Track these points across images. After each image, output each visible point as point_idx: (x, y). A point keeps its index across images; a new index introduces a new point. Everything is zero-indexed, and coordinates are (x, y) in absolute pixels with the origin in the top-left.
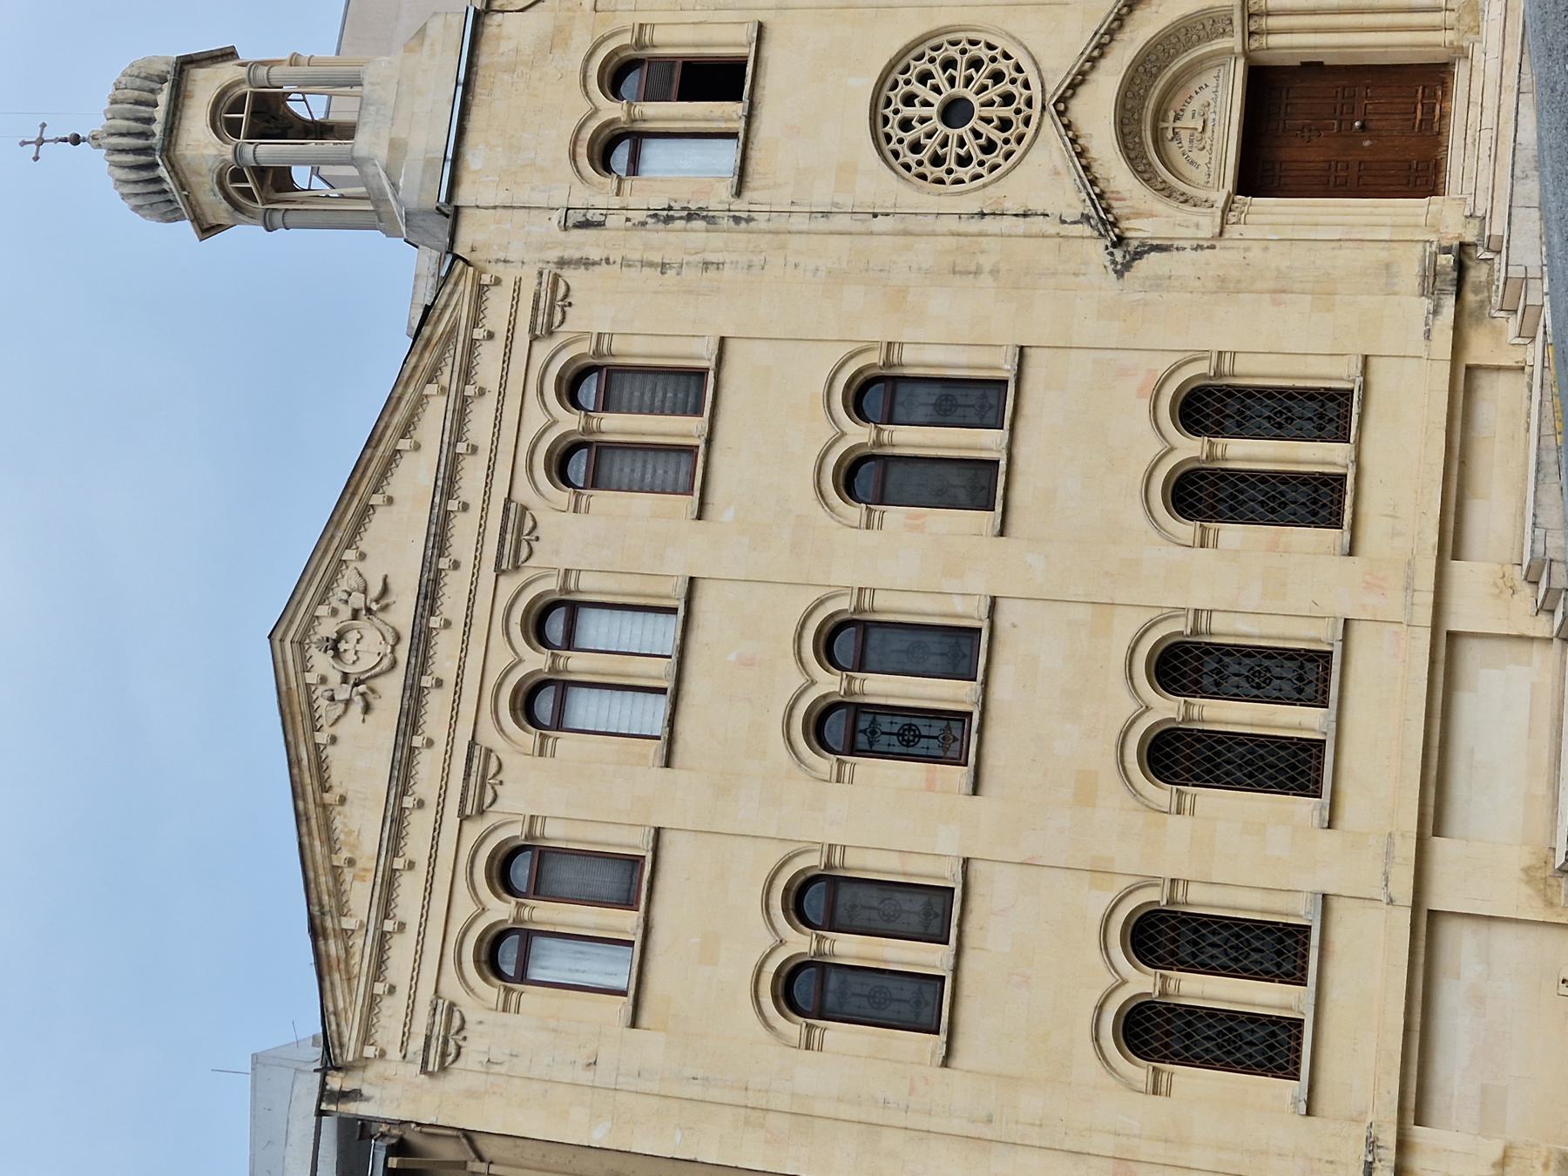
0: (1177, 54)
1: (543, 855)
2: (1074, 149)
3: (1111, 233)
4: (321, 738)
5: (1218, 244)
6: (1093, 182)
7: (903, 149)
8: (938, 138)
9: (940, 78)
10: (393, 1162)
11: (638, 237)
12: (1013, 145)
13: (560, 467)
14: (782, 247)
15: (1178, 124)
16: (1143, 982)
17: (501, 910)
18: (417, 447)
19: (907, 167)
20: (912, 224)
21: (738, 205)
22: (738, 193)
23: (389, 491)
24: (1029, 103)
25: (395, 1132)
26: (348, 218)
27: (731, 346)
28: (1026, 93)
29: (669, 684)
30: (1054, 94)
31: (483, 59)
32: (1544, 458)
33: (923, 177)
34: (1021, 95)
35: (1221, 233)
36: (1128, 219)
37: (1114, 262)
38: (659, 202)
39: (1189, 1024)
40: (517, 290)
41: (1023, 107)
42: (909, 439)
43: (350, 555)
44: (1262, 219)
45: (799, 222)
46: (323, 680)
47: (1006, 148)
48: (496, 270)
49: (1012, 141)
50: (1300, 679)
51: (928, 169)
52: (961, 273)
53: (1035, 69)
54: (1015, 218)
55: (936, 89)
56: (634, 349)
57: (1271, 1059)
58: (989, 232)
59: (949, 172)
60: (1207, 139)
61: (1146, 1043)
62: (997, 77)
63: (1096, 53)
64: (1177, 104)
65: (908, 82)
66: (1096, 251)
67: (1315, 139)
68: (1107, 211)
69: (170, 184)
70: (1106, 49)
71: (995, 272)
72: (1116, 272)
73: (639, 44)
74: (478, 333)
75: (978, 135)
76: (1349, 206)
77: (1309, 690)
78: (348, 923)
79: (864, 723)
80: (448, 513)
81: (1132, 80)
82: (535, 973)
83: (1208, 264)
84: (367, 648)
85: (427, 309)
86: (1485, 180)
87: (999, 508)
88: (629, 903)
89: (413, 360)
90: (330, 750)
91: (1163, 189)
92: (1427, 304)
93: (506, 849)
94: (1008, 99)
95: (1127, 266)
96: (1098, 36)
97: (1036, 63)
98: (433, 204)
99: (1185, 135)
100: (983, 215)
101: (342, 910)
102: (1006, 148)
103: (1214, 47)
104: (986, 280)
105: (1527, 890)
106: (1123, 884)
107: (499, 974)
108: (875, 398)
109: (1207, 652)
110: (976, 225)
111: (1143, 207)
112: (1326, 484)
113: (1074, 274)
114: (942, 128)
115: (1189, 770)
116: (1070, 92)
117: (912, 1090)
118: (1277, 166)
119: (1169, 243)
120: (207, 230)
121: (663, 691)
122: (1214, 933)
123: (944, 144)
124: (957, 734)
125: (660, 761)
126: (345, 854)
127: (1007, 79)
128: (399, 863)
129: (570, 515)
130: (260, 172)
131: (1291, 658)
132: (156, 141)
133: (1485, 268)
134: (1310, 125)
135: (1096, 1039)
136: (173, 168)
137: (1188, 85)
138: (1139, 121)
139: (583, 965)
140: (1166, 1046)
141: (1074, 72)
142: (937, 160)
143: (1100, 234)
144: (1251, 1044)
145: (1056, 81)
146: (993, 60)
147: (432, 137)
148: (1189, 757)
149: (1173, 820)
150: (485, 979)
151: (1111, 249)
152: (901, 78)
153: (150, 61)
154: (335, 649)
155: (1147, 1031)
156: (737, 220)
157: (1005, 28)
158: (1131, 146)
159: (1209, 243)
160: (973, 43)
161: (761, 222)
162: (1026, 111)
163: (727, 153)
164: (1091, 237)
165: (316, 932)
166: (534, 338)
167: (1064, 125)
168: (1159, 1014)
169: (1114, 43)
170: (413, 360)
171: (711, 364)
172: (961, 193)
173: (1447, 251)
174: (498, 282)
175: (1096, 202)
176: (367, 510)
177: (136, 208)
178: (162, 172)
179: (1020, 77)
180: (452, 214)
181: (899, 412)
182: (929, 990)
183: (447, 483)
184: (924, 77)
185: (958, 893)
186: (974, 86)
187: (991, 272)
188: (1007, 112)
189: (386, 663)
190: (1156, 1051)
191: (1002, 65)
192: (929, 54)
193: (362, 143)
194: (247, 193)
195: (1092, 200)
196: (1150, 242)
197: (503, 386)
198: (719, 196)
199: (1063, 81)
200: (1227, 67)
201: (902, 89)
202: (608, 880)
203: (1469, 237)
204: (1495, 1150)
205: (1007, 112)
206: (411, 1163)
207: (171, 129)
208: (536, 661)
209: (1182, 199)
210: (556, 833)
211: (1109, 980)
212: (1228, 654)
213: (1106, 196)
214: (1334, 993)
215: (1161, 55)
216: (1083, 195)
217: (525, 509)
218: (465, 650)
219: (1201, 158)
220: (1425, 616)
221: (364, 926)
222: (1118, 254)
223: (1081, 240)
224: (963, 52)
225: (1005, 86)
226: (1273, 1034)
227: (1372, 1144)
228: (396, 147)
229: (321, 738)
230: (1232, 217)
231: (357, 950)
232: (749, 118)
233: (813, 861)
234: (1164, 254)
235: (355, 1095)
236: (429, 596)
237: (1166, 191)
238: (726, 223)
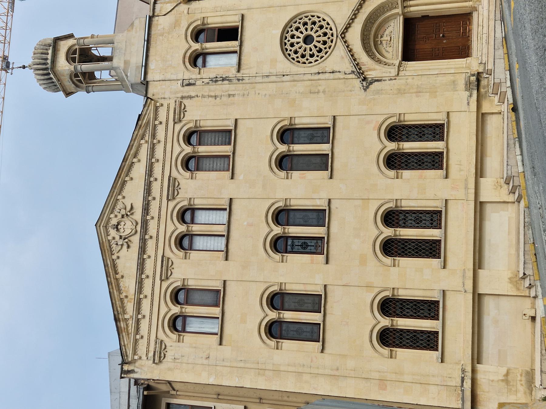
0: (380, 15)
1: (188, 291)
2: (348, 49)
3: (362, 77)
4: (114, 257)
5: (397, 78)
6: (355, 60)
7: (292, 53)
8: (303, 49)
9: (303, 29)
10: (145, 393)
11: (206, 88)
13: (186, 164)
14: (254, 88)
15: (382, 39)
16: (385, 322)
17: (176, 310)
18: (139, 161)
19: (293, 59)
20: (296, 77)
21: (239, 75)
22: (239, 71)
23: (131, 175)
24: (332, 35)
25: (146, 382)
26: (113, 87)
27: (239, 122)
28: (331, 32)
29: (225, 233)
30: (340, 31)
31: (153, 32)
32: (510, 142)
33: (299, 62)
34: (329, 33)
35: (398, 74)
36: (367, 71)
37: (363, 86)
38: (213, 75)
39: (401, 335)
40: (168, 107)
41: (330, 36)
42: (299, 148)
43: (120, 197)
44: (411, 69)
45: (259, 79)
46: (114, 238)
47: (325, 50)
48: (162, 101)
49: (327, 48)
50: (432, 220)
51: (300, 59)
52: (313, 93)
53: (333, 24)
54: (330, 74)
55: (302, 33)
56: (208, 124)
57: (428, 345)
58: (322, 79)
59: (307, 59)
60: (392, 43)
61: (387, 342)
62: (321, 27)
63: (353, 17)
64: (381, 32)
65: (292, 31)
66: (357, 83)
67: (427, 41)
68: (360, 69)
69: (55, 80)
70: (357, 16)
71: (324, 92)
72: (364, 89)
73: (203, 24)
74: (157, 122)
75: (316, 47)
76: (440, 63)
77: (435, 223)
78: (127, 316)
79: (290, 242)
80: (150, 182)
81: (366, 25)
82: (188, 329)
83: (394, 85)
84: (127, 227)
85: (140, 115)
86: (485, 51)
87: (330, 170)
88: (217, 305)
89: (136, 132)
90: (117, 261)
91: (378, 61)
92: (468, 93)
93: (176, 290)
94: (325, 34)
95: (368, 87)
96: (354, 11)
97: (334, 22)
98: (139, 81)
99: (384, 42)
100: (319, 73)
101: (124, 312)
102: (325, 50)
103: (392, 13)
104: (321, 95)
105: (510, 285)
106: (377, 290)
107: (177, 330)
108: (287, 136)
109: (401, 213)
110: (317, 77)
111: (372, 67)
112: (437, 155)
113: (350, 91)
114: (304, 45)
115: (397, 252)
116: (346, 30)
117: (312, 361)
118: (416, 51)
119: (381, 78)
120: (68, 94)
121: (223, 236)
122: (408, 305)
123: (305, 50)
124: (320, 244)
125: (224, 258)
126: (124, 294)
127: (324, 28)
128: (142, 296)
129: (190, 180)
130: (84, 74)
131: (428, 213)
132: (49, 66)
133: (486, 80)
134: (425, 37)
135: (371, 341)
136: (55, 75)
137: (384, 26)
138: (369, 39)
139: (203, 326)
140: (394, 342)
141: (346, 23)
142: (303, 56)
143: (358, 77)
144: (422, 340)
145: (340, 28)
147: (137, 59)
148: (396, 248)
149: (392, 269)
150: (172, 332)
151: (362, 82)
152: (290, 30)
153: (45, 40)
154: (117, 228)
155: (387, 338)
156: (239, 80)
157: (324, 11)
158: (367, 47)
159: (394, 78)
160: (313, 16)
161: (246, 80)
163: (234, 59)
164: (355, 78)
165: (117, 320)
166: (175, 123)
167: (344, 42)
168: (391, 332)
169: (359, 13)
170: (136, 132)
171: (232, 128)
172: (312, 66)
173: (473, 75)
174: (162, 105)
175: (356, 66)
176: (124, 183)
177: (45, 88)
178: (52, 76)
179: (329, 27)
180: (146, 84)
181: (296, 140)
182: (315, 328)
183: (150, 172)
184: (297, 29)
185: (323, 296)
186: (314, 30)
187: (323, 92)
188: (325, 38)
189: (133, 231)
190: (390, 344)
191: (323, 23)
192: (298, 21)
193: (116, 62)
194: (80, 81)
195: (355, 66)
196: (374, 79)
197: (166, 139)
198: (232, 73)
199: (343, 27)
200: (397, 19)
201: (290, 33)
202: (209, 298)
203: (480, 71)
204: (504, 371)
205: (325, 38)
206: (152, 393)
207: (54, 61)
208: (182, 228)
209: (384, 64)
210: (192, 284)
211: (374, 322)
212: (408, 213)
213: (359, 64)
214: (448, 323)
215: (375, 17)
216: (352, 64)
217: (175, 179)
218: (159, 226)
219: (389, 50)
220: (472, 197)
221: (132, 317)
222: (364, 83)
223: (352, 79)
224: (310, 19)
225: (324, 30)
226: (429, 337)
227: (463, 371)
228: (126, 63)
229: (114, 257)
230: (401, 69)
231: (130, 325)
232: (241, 46)
233: (276, 288)
234: (379, 82)
235: (132, 371)
236: (146, 209)
237: (379, 61)
238: (235, 81)
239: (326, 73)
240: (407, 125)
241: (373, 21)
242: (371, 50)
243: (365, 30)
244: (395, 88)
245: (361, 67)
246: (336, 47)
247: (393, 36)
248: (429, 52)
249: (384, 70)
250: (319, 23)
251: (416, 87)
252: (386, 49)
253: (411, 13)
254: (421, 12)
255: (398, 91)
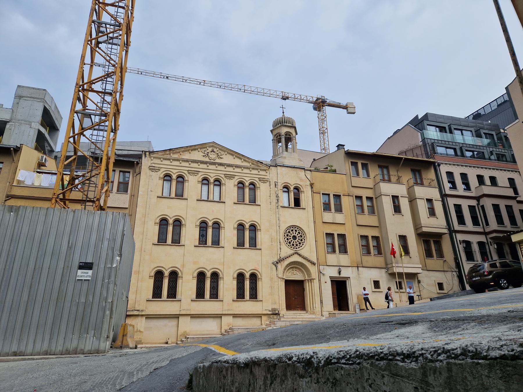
1: (183, 182)
4: (199, 150)
6: (285, 258)
7: (289, 230)
8: (291, 235)
9: (299, 235)
10: (135, 162)
11: (274, 192)
12: (290, 246)
13: (240, 183)
14: (274, 213)
16: (167, 273)
17: (174, 177)
18: (242, 162)
19: (286, 231)
20: (278, 232)
21: (279, 207)
22: (281, 207)
23: (236, 158)
24: (296, 248)
25: (140, 162)
26: (274, 151)
27: (259, 206)
29: (209, 200)
31: (298, 169)
32: (249, 329)
33: (285, 233)
37: (274, 262)
38: (279, 195)
39: (160, 281)
40: (265, 176)
42: (247, 233)
43: (226, 153)
44: (282, 284)
45: (277, 216)
46: (208, 150)
48: (268, 173)
50: (214, 294)
51: (286, 234)
55: (297, 235)
56: (258, 193)
57: (155, 294)
59: (286, 237)
61: (157, 275)
62: (300, 243)
64: (297, 270)
65: (298, 230)
66: (276, 259)
68: (282, 261)
69: (278, 126)
71: (272, 245)
73: (301, 192)
74: (259, 170)
75: (291, 241)
77: (212, 296)
78: (171, 154)
79: (204, 229)
80: (233, 167)
82: (165, 182)
84: (213, 156)
85: (262, 163)
86: (289, 317)
87: (237, 247)
88: (176, 195)
89: (255, 161)
90: (197, 151)
92: (270, 309)
93: (183, 177)
94: (297, 245)
95: (274, 264)
98: (277, 163)
99: (293, 271)
101: (173, 153)
104: (271, 243)
105: (183, 332)
106: (181, 269)
107: (165, 177)
108: (252, 228)
109: (217, 280)
110: (278, 241)
112: (243, 296)
114: (292, 236)
115: (199, 278)
117: (149, 239)
120: (272, 131)
121: (208, 199)
122: (174, 284)
123: (290, 236)
124: (203, 243)
125: (198, 199)
126: (182, 154)
128: (181, 161)
129: (234, 184)
130: (280, 139)
131: (217, 293)
132: (284, 124)
133: (276, 318)
135: (158, 267)
136: (280, 126)
138: (295, 265)
139: (166, 189)
140: (157, 278)
142: (287, 235)
144: (157, 291)
145: (300, 252)
146: (302, 243)
147: (287, 162)
148: (201, 278)
149: (192, 276)
150: (164, 175)
152: (299, 229)
153: (295, 123)
154: (212, 151)
155: (159, 275)
156: (277, 207)
160: (304, 240)
161: (277, 210)
162: (295, 248)
163: (286, 205)
165: (170, 150)
166: (259, 178)
168: (162, 276)
170: (255, 161)
171: (256, 204)
173: (278, 312)
174: (267, 173)
176: (233, 155)
177: (274, 121)
178: (280, 125)
180: (276, 166)
181: (251, 232)
182: (164, 241)
183: (237, 166)
184: (299, 233)
185: (179, 244)
186: (298, 240)
188: (295, 245)
189: (211, 159)
190: (156, 276)
191: (302, 244)
192: (303, 233)
193: (285, 153)
194: (277, 137)
197: (252, 174)
198: (281, 204)
201: (297, 230)
202: (180, 192)
203: (280, 315)
204: (142, 330)
205: (295, 245)
206: (135, 165)
207: (286, 126)
208: (212, 180)
210: (186, 184)
211: (167, 268)
212: (217, 283)
214: (165, 303)
217: (234, 178)
218: (213, 170)
219: (290, 274)
220: (224, 313)
221: (171, 156)
222: (275, 263)
224: (303, 238)
225: (298, 245)
226: (159, 294)
227: (142, 311)
228: (285, 158)
229: (199, 150)
231: (167, 156)
232: (292, 208)
233: (183, 222)
235: (145, 156)
236: (221, 164)
237: (285, 269)
238: (277, 205)
240: (257, 282)
249: (281, 271)
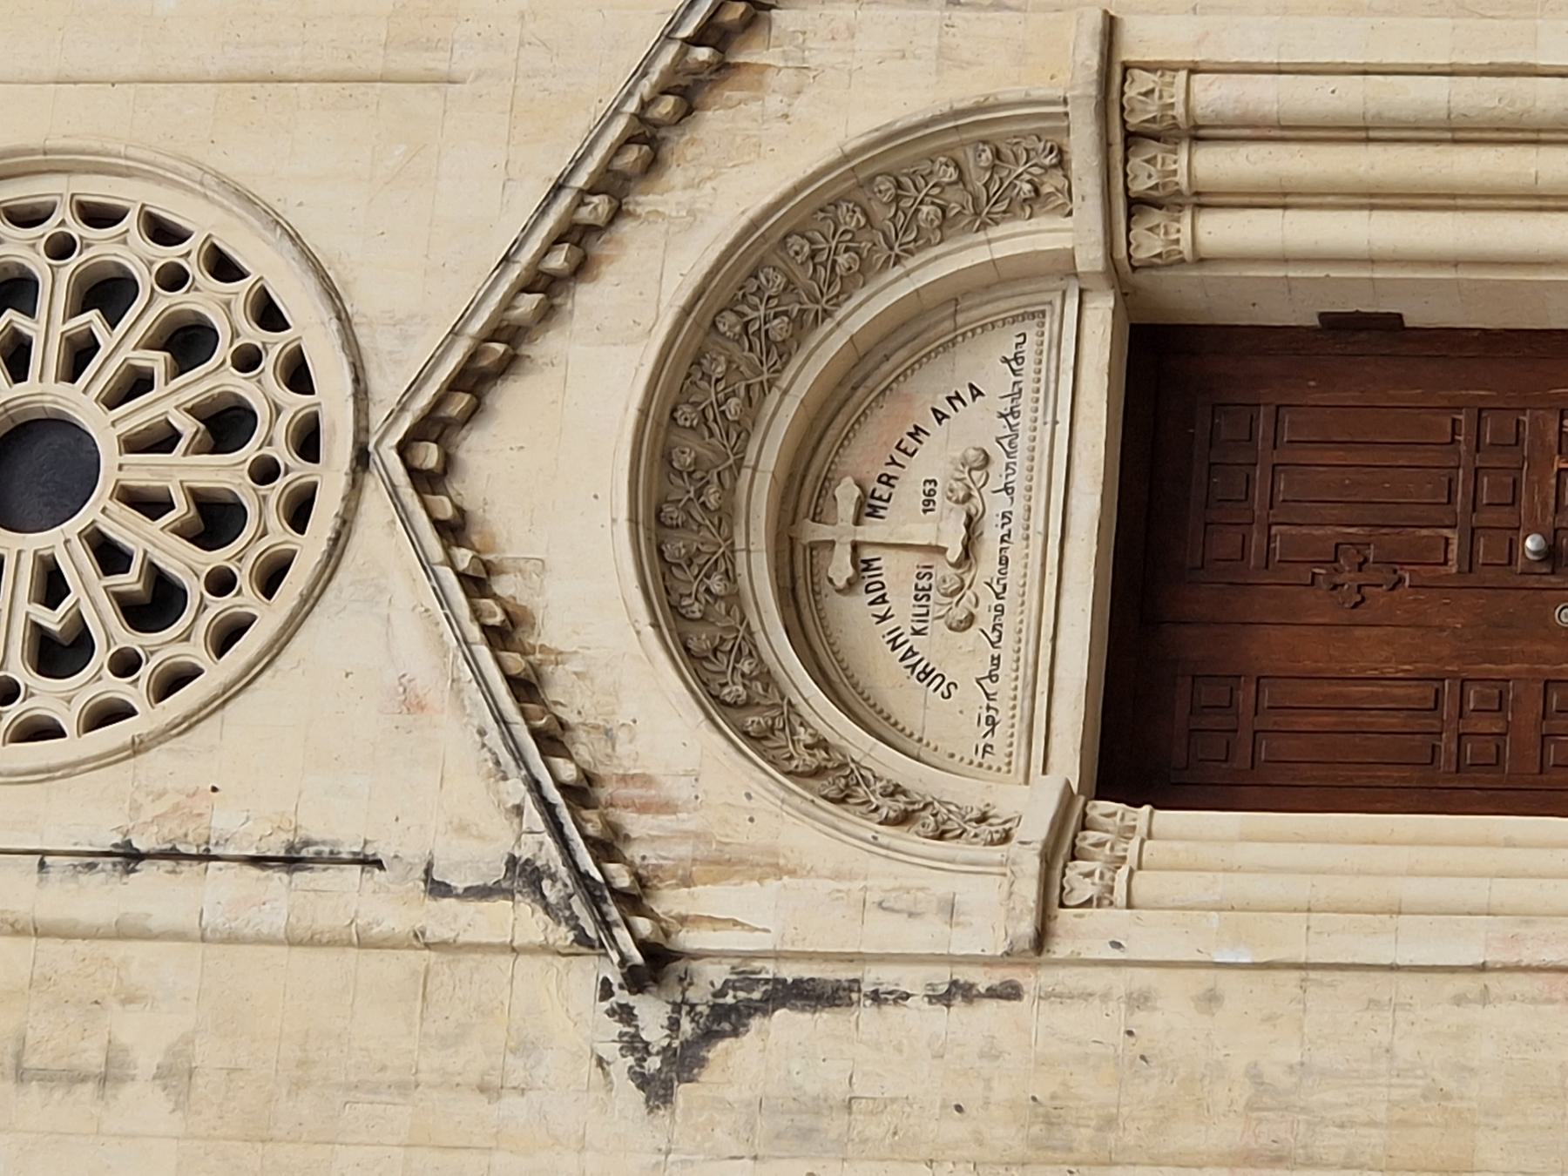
0: (864, 271)
2: (476, 614)
3: (622, 934)
5: (1028, 980)
15: (872, 531)
24: (308, 442)
28: (295, 403)
30: (403, 407)
34: (277, 410)
35: (1041, 939)
36: (687, 881)
37: (635, 1045)
41: (283, 453)
47: (219, 606)
49: (243, 580)
52: (47, 1077)
53: (327, 315)
54: (253, 872)
58: (154, 924)
60: (980, 587)
63: (558, 261)
67: (1379, 597)
68: (606, 847)
70: (598, 248)
72: (643, 1081)
75: (110, 556)
81: (697, 362)
83: (992, 1053)
91: (818, 772)
96: (565, 199)
97: (331, 293)
99: (896, 571)
100: (129, 857)
102: (219, 606)
103: (1002, 250)
111: (743, 836)
113: (483, 1089)
116: (461, 401)
118: (1246, 695)
119: (843, 973)
127: (224, 351)
134: (1360, 545)
137: (905, 387)
138: (725, 516)
141: (476, 326)
143: (582, 939)
151: (622, 996)
158: (696, 610)
159: (995, 977)
160: (100, 216)
164: (545, 949)
167: (440, 526)
169: (626, 227)
172: (49, 774)
175: (565, 815)
179: (274, 345)
186: (103, 371)
187: (163, 1075)
195: (548, 809)
196: (770, 970)
199: (435, 361)
200: (1051, 326)
209: (890, 808)
213: (603, 793)
215: (803, 276)
216: (516, 790)
222: (652, 1014)
223: (506, 960)
224: (61, 248)
230: (1079, 880)
239: (206, 857)
241: (778, 326)
242: (746, 647)
243: (686, 414)
244: (1001, 1091)
245: (614, 829)
246: (340, 576)
247: (996, 505)
248: (1393, 721)
249: (882, 875)
250: (169, 301)
251: (1243, 1093)
252: (915, 641)
253: (1207, 272)
254: (1318, 273)
255: (1036, 1130)
